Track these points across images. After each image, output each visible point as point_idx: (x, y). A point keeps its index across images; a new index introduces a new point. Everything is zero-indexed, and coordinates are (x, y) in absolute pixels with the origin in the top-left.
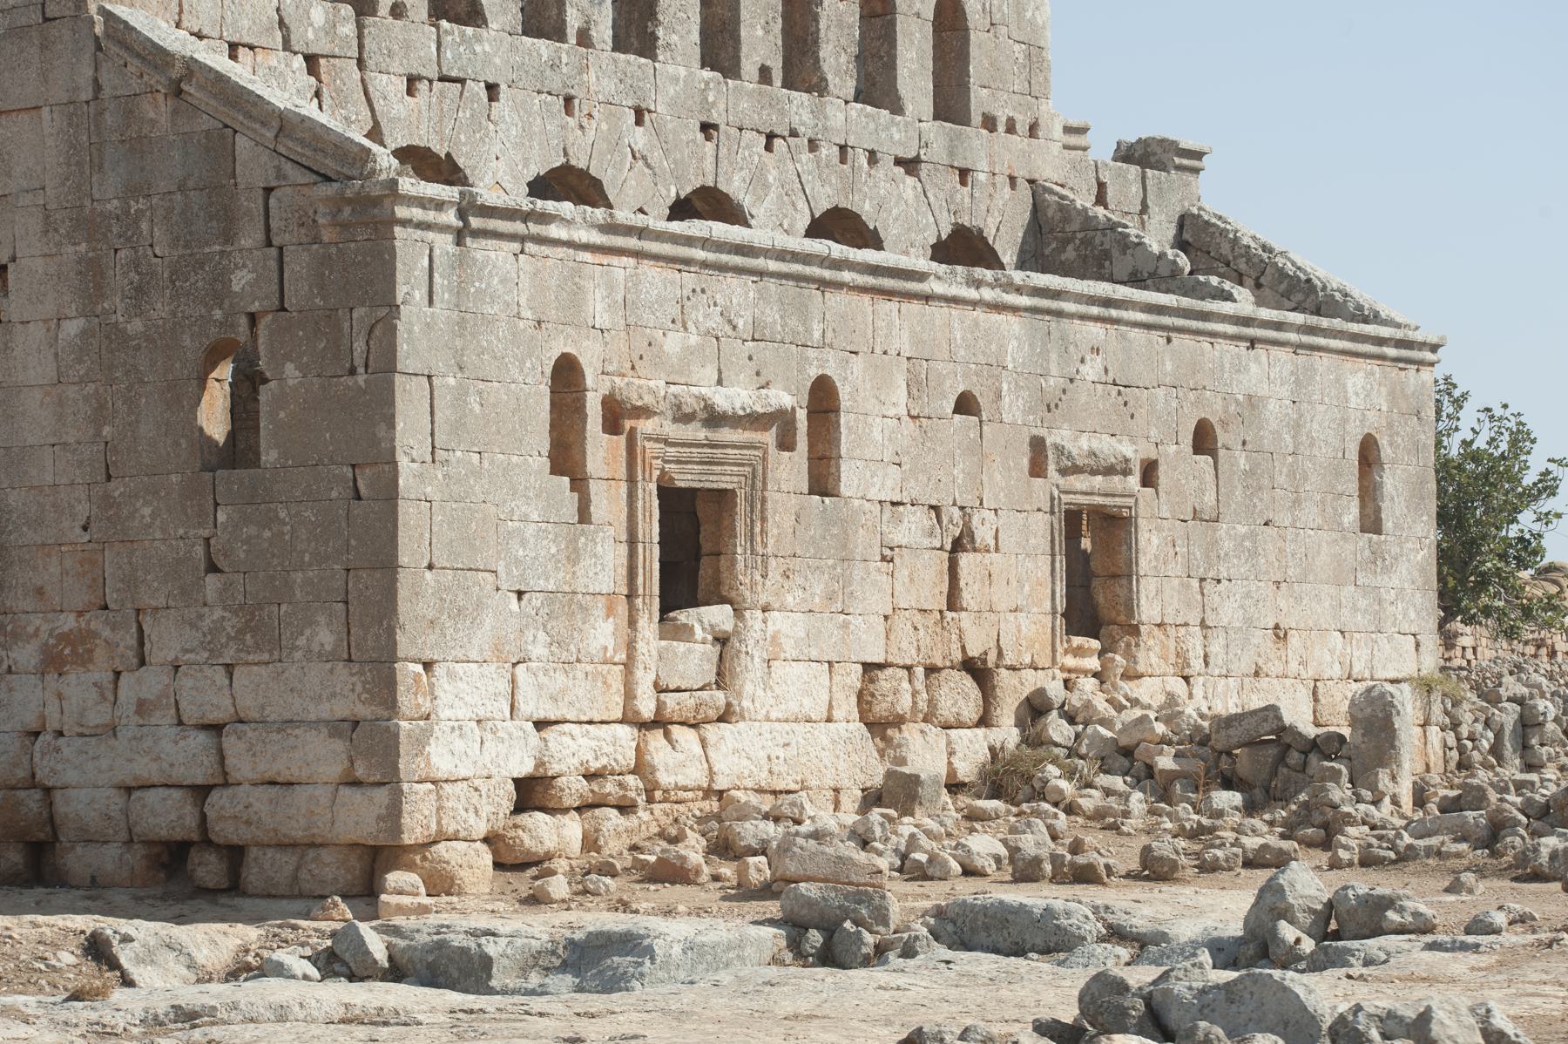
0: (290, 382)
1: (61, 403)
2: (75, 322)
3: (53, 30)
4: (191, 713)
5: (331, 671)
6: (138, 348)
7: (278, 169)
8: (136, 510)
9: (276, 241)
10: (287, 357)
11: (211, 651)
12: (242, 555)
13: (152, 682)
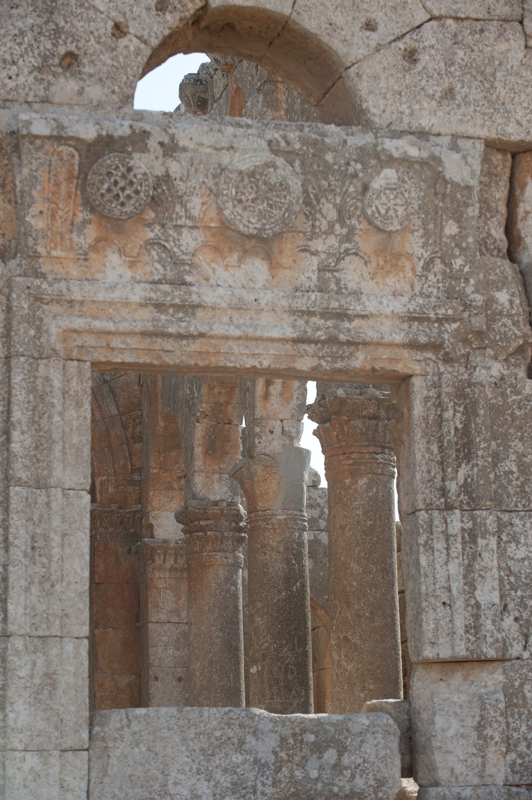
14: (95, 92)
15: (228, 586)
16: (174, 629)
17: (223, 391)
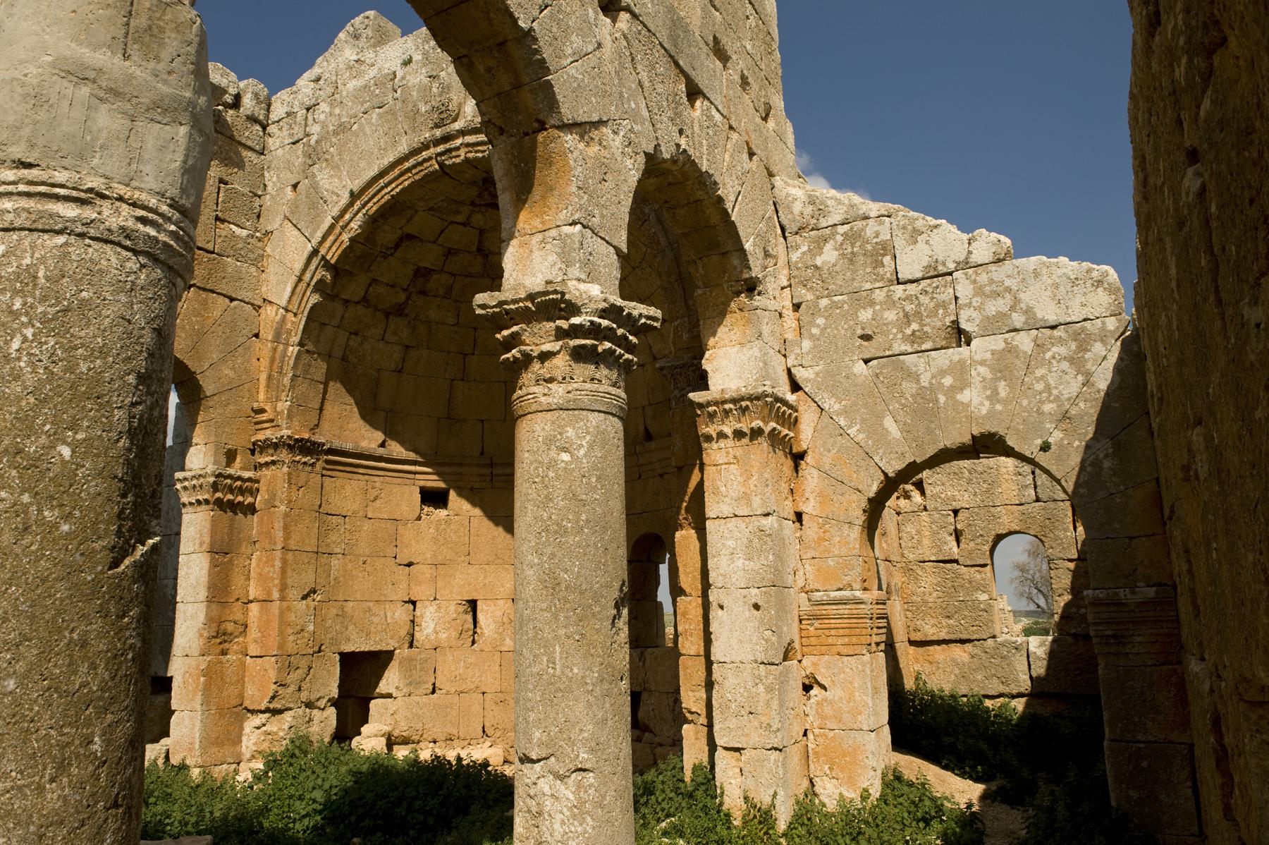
15: (553, 454)
16: (743, 525)
17: (492, 63)
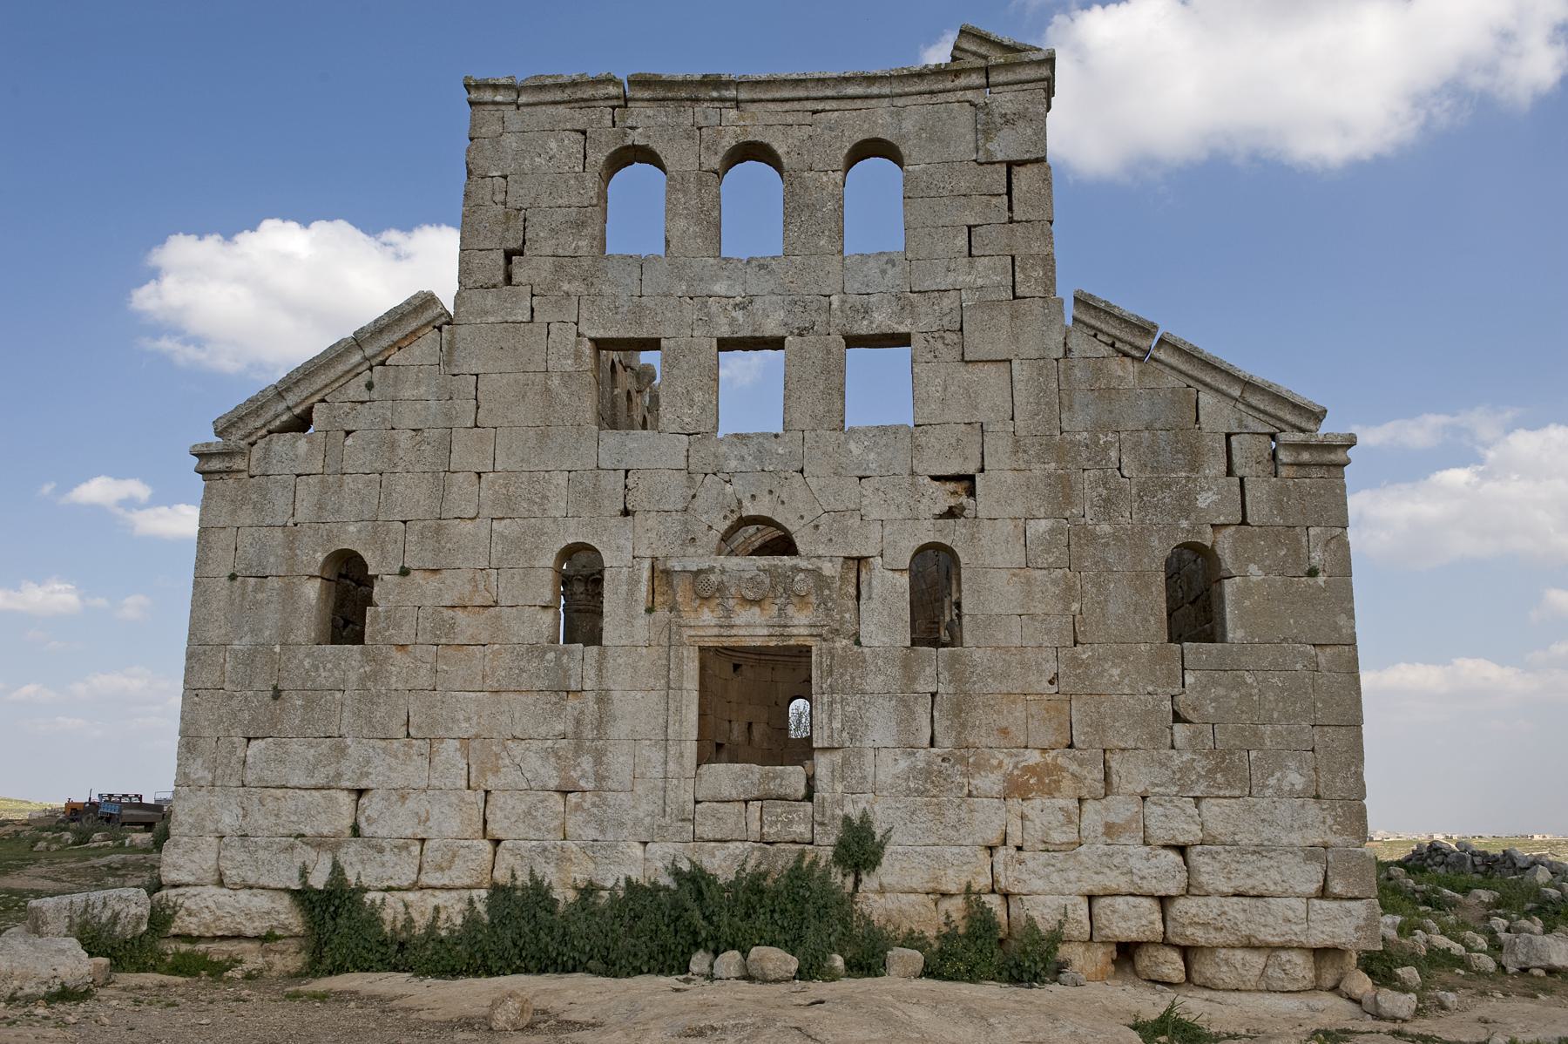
0: (1254, 579)
1: (1028, 582)
2: (1043, 522)
3: (1023, 306)
4: (1159, 834)
5: (1303, 806)
6: (1108, 544)
7: (1240, 422)
8: (1104, 670)
9: (1239, 472)
10: (1250, 560)
11: (1182, 786)
12: (1212, 711)
13: (1121, 808)
14: (700, 551)
